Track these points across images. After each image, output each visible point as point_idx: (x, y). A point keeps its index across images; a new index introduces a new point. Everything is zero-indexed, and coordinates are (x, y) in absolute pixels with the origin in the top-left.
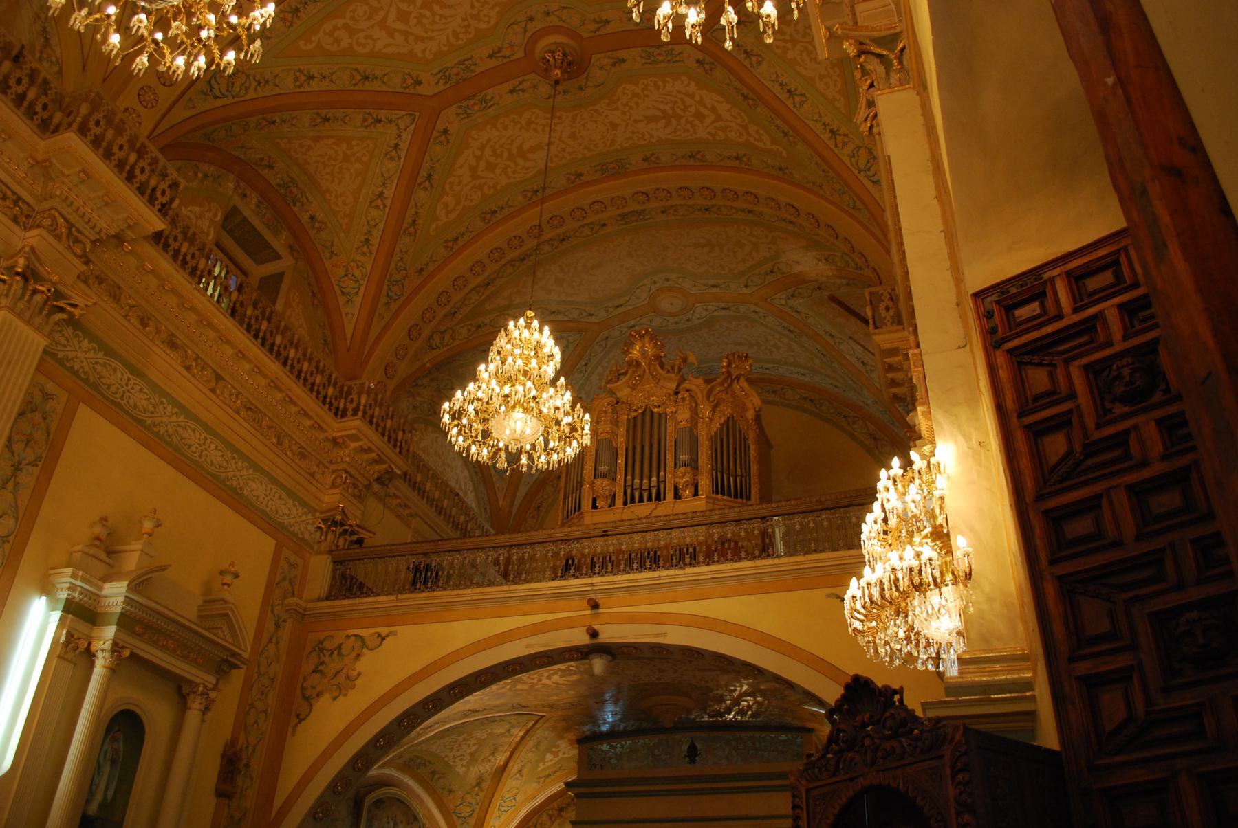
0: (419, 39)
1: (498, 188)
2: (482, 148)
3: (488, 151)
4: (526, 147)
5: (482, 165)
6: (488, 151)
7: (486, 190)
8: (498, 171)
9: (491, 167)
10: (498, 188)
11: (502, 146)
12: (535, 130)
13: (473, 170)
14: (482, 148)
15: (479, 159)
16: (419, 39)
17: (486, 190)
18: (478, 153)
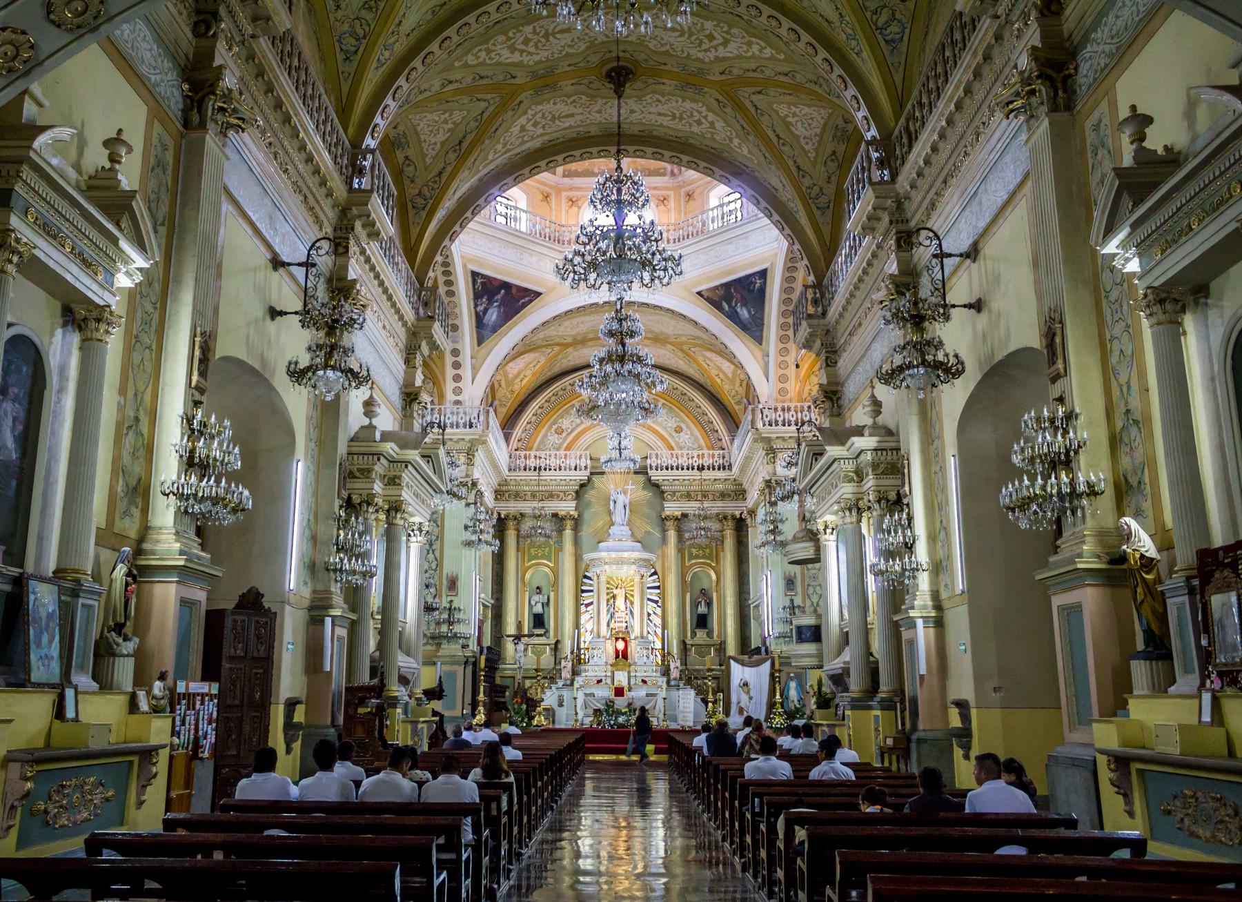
0: (700, 113)
1: (715, 23)
2: (706, 51)
3: (704, 47)
4: (678, 33)
5: (715, 43)
6: (704, 47)
7: (726, 29)
8: (707, 32)
9: (711, 37)
10: (715, 23)
11: (692, 43)
12: (662, 39)
13: (726, 43)
14: (707, 50)
15: (716, 48)
16: (700, 113)
17: (726, 29)
18: (712, 50)
